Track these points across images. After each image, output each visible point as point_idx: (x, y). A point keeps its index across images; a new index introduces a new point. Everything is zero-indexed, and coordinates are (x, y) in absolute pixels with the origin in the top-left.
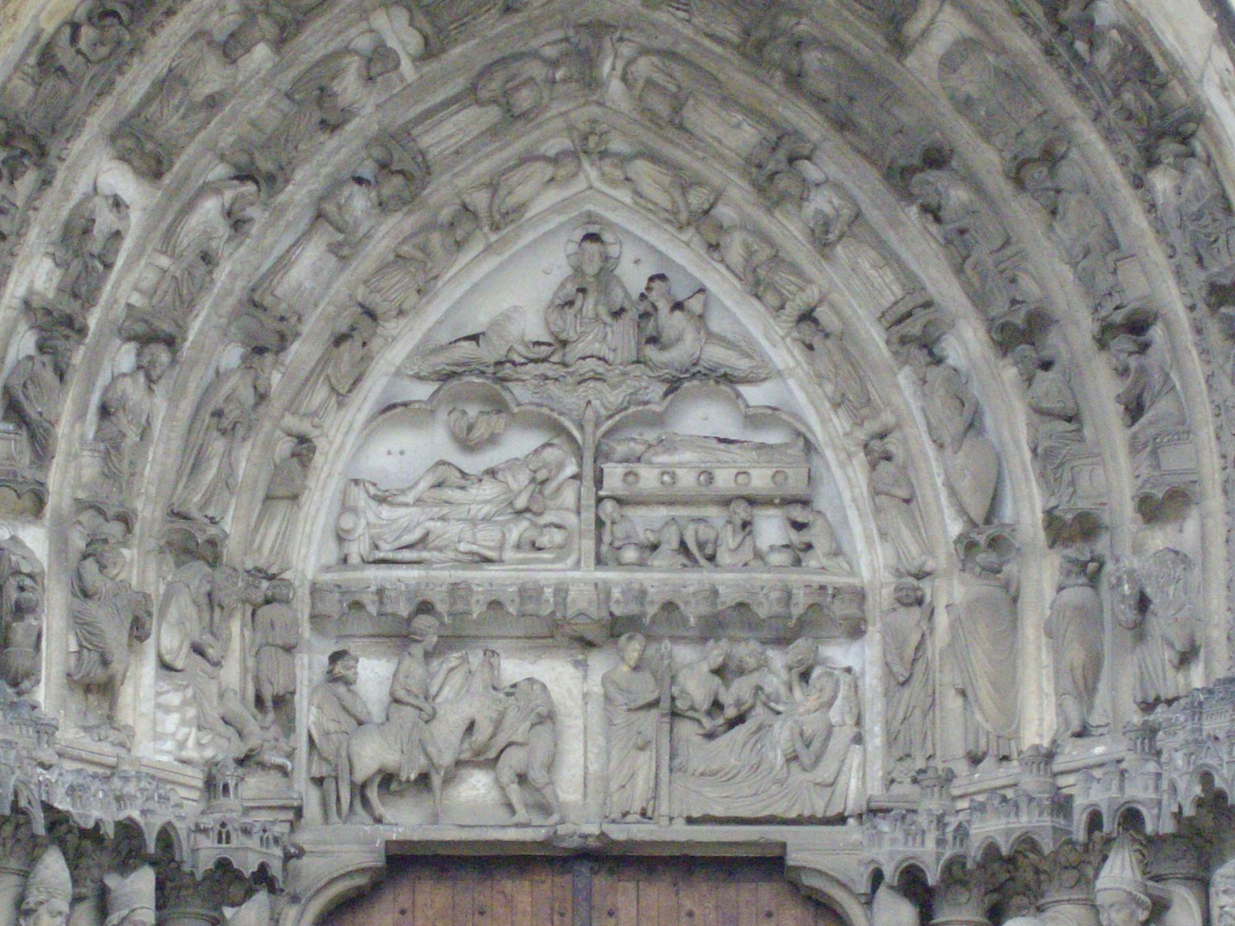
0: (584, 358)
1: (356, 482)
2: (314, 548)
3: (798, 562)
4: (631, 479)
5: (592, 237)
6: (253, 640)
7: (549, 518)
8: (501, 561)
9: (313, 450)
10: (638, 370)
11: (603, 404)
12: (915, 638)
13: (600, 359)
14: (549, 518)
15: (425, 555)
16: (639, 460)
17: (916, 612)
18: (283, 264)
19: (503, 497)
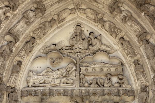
0: (77, 48)
1: (31, 71)
2: (22, 83)
3: (121, 86)
4: (86, 70)
5: (79, 26)
6: (8, 100)
7: (70, 78)
8: (60, 86)
9: (22, 63)
10: (88, 51)
11: (81, 57)
12: (145, 98)
13: (80, 48)
14: (70, 78)
15: (44, 85)
16: (88, 67)
17: (145, 93)
18: (16, 25)
19: (60, 74)
